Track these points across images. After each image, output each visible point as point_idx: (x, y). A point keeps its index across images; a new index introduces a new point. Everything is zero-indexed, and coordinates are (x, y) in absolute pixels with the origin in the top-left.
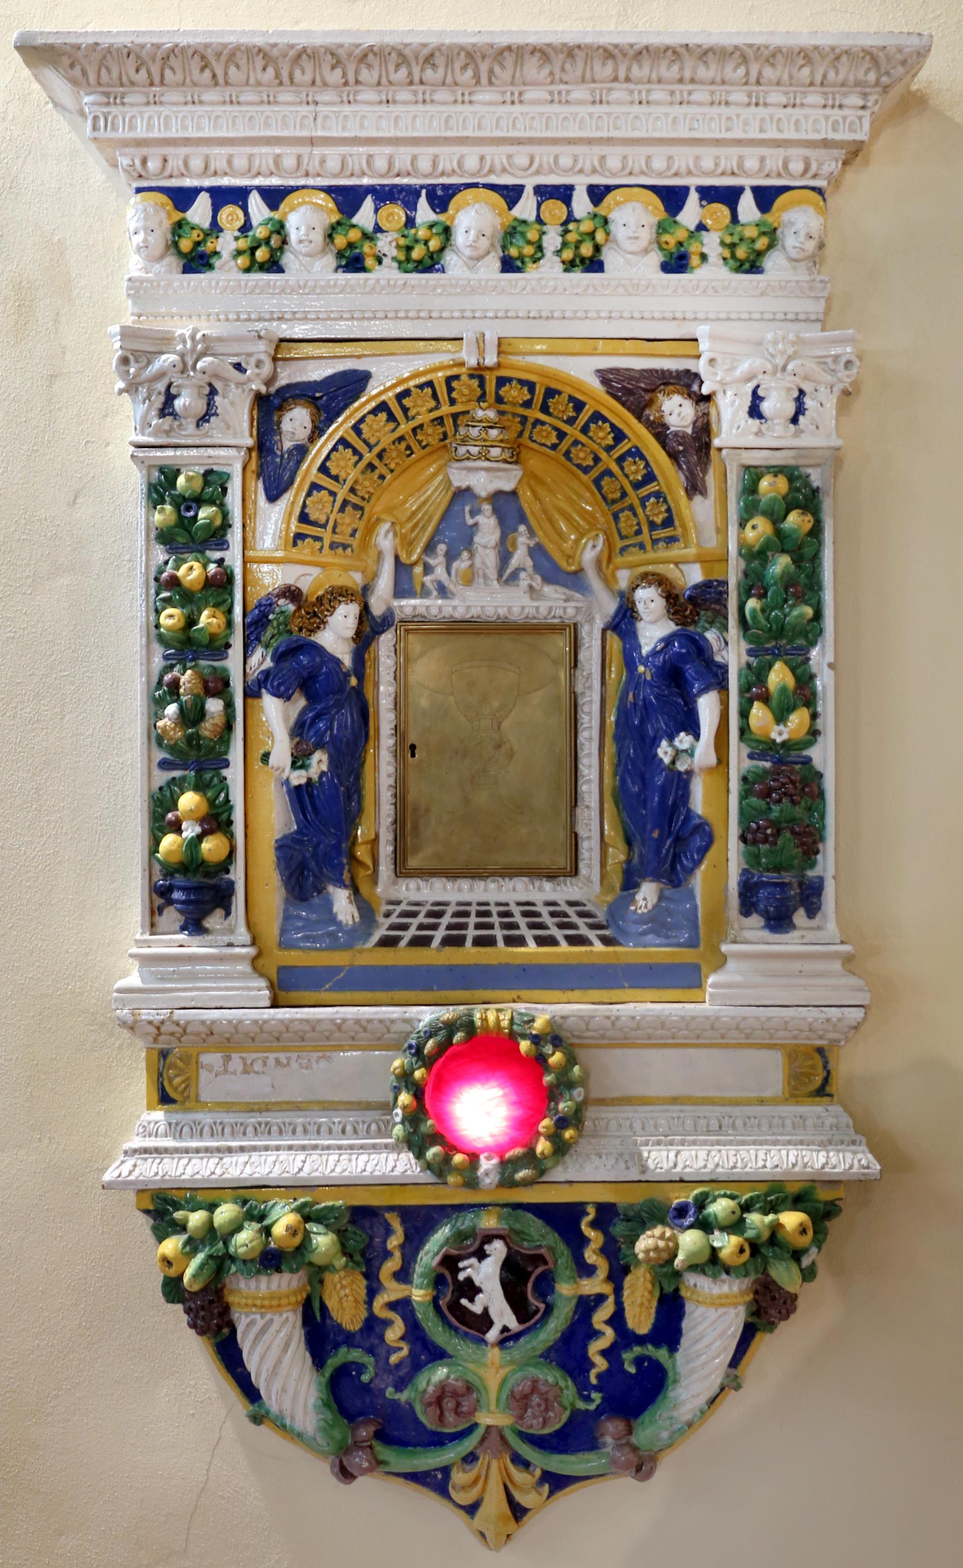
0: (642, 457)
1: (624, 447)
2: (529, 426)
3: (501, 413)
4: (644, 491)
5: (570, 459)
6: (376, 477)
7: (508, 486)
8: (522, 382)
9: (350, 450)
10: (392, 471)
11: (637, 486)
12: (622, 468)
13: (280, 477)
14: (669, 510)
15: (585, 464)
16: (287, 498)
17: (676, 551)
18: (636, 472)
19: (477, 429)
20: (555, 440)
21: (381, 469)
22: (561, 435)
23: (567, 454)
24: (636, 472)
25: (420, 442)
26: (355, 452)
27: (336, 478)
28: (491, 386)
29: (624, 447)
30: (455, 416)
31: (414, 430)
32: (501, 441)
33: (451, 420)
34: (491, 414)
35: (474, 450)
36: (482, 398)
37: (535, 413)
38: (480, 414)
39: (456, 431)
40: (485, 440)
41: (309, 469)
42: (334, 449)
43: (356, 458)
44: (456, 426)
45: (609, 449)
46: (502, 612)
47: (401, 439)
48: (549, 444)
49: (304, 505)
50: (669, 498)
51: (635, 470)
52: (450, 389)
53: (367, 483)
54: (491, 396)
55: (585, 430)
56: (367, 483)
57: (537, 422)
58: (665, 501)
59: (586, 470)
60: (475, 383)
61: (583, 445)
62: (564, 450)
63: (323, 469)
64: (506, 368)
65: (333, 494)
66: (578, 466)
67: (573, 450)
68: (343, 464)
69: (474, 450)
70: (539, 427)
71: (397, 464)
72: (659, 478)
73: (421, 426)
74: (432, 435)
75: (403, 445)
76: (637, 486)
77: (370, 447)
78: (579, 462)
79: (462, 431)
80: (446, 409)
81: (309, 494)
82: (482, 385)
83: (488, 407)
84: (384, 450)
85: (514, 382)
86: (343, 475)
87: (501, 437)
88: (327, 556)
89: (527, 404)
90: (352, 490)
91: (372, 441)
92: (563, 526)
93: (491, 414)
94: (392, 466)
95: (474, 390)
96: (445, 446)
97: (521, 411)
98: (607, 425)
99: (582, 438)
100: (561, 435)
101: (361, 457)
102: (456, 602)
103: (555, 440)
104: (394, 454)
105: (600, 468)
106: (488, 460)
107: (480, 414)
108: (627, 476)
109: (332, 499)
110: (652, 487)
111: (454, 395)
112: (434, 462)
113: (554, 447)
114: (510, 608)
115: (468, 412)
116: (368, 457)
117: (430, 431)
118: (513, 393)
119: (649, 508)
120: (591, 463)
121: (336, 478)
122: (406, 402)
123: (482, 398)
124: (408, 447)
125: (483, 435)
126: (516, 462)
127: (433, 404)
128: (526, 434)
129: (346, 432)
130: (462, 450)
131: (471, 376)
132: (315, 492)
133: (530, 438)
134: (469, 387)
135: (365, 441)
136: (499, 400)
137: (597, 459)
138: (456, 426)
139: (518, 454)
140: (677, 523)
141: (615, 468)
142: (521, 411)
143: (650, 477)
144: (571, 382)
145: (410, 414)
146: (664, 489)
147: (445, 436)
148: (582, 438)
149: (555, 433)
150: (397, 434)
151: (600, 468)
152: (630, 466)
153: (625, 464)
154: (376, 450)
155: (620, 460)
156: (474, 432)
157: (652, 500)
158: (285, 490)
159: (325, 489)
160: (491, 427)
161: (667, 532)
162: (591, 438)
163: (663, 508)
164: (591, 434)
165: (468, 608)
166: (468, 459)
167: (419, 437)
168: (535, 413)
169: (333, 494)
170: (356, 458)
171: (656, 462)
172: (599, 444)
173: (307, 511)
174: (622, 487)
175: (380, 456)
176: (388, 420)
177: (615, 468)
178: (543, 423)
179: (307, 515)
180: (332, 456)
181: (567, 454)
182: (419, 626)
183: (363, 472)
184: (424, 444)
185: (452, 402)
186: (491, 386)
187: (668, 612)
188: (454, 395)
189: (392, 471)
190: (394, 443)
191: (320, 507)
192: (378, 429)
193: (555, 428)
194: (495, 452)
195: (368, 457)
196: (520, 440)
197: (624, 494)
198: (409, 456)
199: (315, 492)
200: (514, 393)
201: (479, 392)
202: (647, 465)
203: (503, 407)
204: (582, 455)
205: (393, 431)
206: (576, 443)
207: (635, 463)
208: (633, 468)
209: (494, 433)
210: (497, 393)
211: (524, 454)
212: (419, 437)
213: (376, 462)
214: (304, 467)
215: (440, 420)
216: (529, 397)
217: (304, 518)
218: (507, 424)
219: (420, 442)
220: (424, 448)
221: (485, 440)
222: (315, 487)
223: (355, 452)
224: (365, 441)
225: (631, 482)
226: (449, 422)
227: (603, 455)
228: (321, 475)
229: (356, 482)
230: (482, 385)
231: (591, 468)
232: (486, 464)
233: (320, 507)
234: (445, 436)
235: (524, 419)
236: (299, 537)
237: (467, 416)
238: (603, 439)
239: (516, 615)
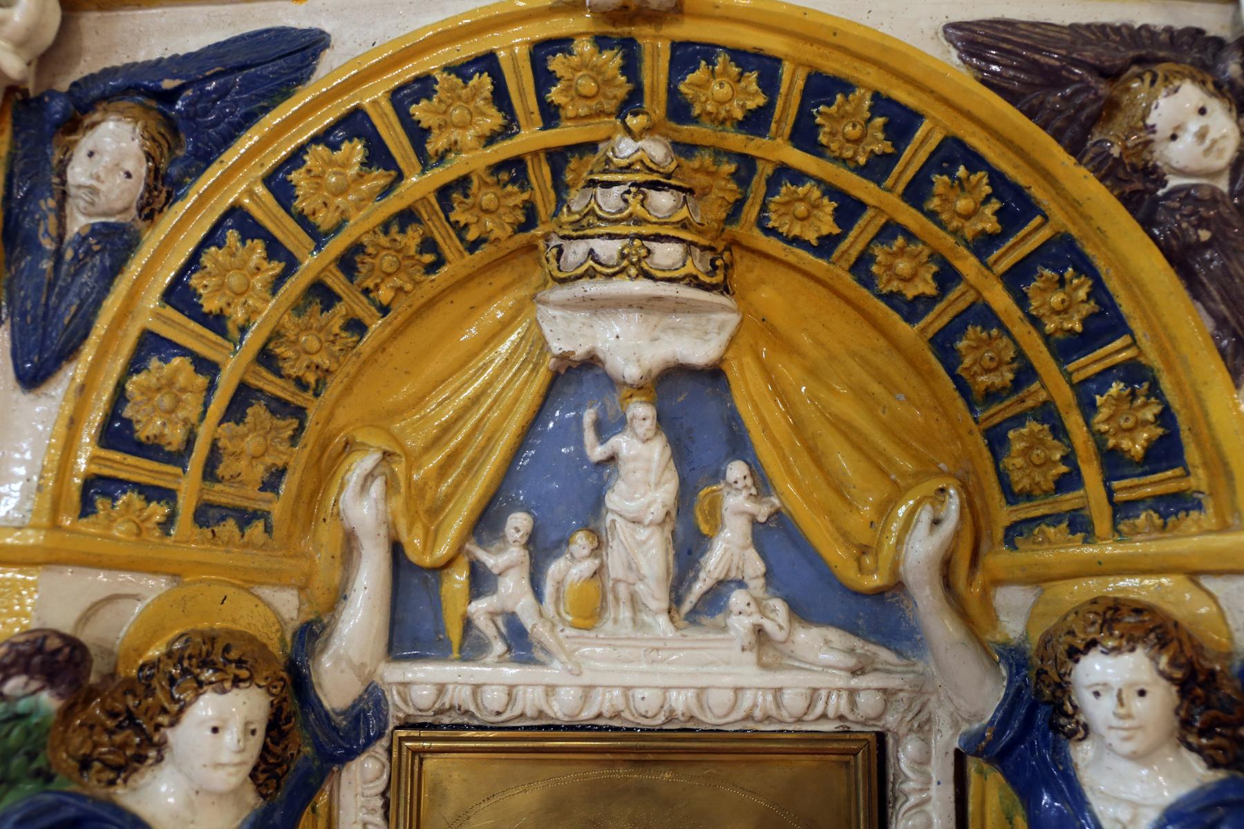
0: (1085, 267)
1: (1033, 237)
2: (758, 186)
3: (683, 149)
4: (1088, 365)
5: (867, 281)
6: (336, 325)
7: (698, 348)
8: (744, 58)
9: (259, 248)
10: (384, 310)
11: (1067, 348)
12: (1022, 301)
13: (48, 316)
14: (1166, 417)
15: (910, 293)
16: (74, 372)
17: (1193, 539)
18: (1064, 311)
19: (616, 191)
20: (828, 226)
21: (352, 303)
22: (849, 210)
23: (861, 267)
24: (1064, 311)
25: (460, 230)
26: (275, 249)
27: (216, 322)
28: (655, 72)
29: (1033, 237)
30: (558, 158)
31: (444, 193)
32: (684, 225)
33: (546, 170)
34: (656, 150)
35: (608, 249)
36: (632, 102)
37: (778, 149)
38: (626, 148)
39: (561, 202)
40: (639, 221)
41: (137, 298)
42: (213, 238)
43: (276, 267)
44: (560, 187)
45: (983, 246)
46: (681, 702)
47: (407, 217)
48: (811, 236)
49: (120, 396)
50: (1166, 384)
51: (1063, 303)
52: (544, 79)
53: (309, 341)
54: (656, 104)
55: (916, 193)
56: (309, 341)
57: (785, 174)
58: (1155, 391)
59: (912, 309)
60: (612, 60)
61: (910, 237)
62: (854, 254)
63: (179, 295)
64: (701, 16)
65: (205, 367)
66: (891, 299)
67: (880, 253)
68: (240, 283)
69: (608, 249)
70: (786, 188)
71: (399, 290)
72: (1136, 325)
73: (463, 183)
74: (492, 213)
75: (412, 239)
76: (1067, 348)
77: (318, 237)
78: (895, 286)
79: (577, 201)
80: (531, 137)
81: (136, 365)
82: (631, 68)
83: (649, 130)
84: (357, 248)
85: (722, 59)
86: (239, 315)
87: (683, 213)
88: (187, 540)
89: (756, 122)
90: (266, 358)
91: (324, 219)
92: (844, 460)
93: (656, 150)
94: (385, 295)
95: (609, 82)
96: (531, 247)
97: (737, 141)
98: (981, 177)
99: (909, 217)
100: (849, 210)
101: (292, 265)
102: (553, 672)
103: (828, 226)
104: (387, 261)
105: (957, 301)
106: (647, 275)
107: (626, 148)
108: (1036, 322)
109: (201, 381)
110: (1115, 351)
111: (555, 95)
112: (505, 289)
113: (825, 246)
114: (701, 691)
115: (592, 147)
116: (312, 263)
117: (488, 198)
118: (719, 90)
119: (1104, 413)
120: (925, 286)
121: (216, 322)
122: (418, 111)
123: (632, 102)
124: (429, 245)
125: (635, 207)
126: (724, 289)
127: (493, 119)
128: (751, 212)
129: (250, 193)
130: (576, 252)
131: (602, 42)
132: (154, 363)
133: (761, 223)
134: (597, 70)
135: (302, 220)
136: (679, 110)
137: (947, 277)
138: (560, 187)
139: (728, 267)
140: (1192, 454)
141: (1000, 299)
142: (737, 141)
143: (1106, 322)
144: (882, 56)
145: (430, 148)
146: (1152, 358)
147: (530, 218)
148: (909, 217)
149: (829, 206)
150: (394, 204)
151: (957, 301)
152: (1047, 297)
153: (1032, 288)
154: (337, 246)
155: (1016, 279)
156: (609, 201)
157: (1116, 388)
158: (69, 352)
159: (184, 351)
160: (655, 186)
161: (1163, 482)
162: (932, 215)
163: (1149, 414)
164: (934, 204)
165: (588, 689)
166: (591, 274)
167: (459, 216)
168: (778, 149)
169: (205, 367)
170: (276, 267)
171: (1133, 283)
172: (954, 233)
173: (128, 412)
174: (1020, 355)
175: (348, 263)
176: (368, 163)
177: (1000, 299)
178: (798, 177)
179: (128, 423)
180: (205, 260)
181: (861, 267)
182: (447, 727)
183: (298, 309)
184: (472, 235)
185: (550, 115)
186: (655, 72)
187: (1186, 724)
188: (555, 95)
189: (384, 310)
190: (386, 227)
191: (166, 401)
192: (340, 188)
193: (832, 191)
194: (666, 254)
195: (312, 263)
196: (734, 229)
197: (1026, 373)
198: (432, 268)
199: (154, 363)
200: (720, 90)
201: (622, 87)
202: (1099, 290)
203: (687, 132)
204: (903, 266)
205: (386, 192)
206: (890, 230)
207: (1062, 282)
208: (1056, 299)
209: (663, 201)
210: (673, 92)
211: (746, 270)
212: (459, 216)
213: (336, 281)
214: (122, 286)
215: (514, 168)
216: (761, 100)
217: (117, 434)
218: (701, 180)
219: (460, 230)
220: (473, 247)
221: (639, 221)
222: (153, 344)
223: (275, 249)
224: (302, 220)
225: (1047, 338)
226: (540, 174)
227: (968, 265)
228: (169, 312)
229: (276, 335)
230: (631, 68)
231: (927, 302)
232: (642, 287)
233: (166, 401)
234: (530, 218)
235: (747, 164)
236: (98, 488)
237: (592, 160)
238: (967, 217)
239: (718, 712)
